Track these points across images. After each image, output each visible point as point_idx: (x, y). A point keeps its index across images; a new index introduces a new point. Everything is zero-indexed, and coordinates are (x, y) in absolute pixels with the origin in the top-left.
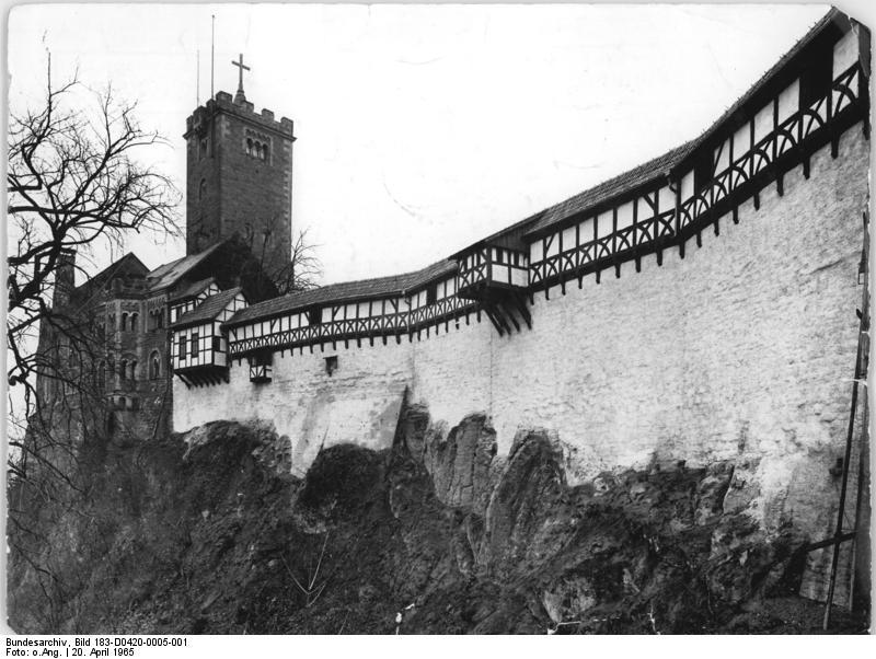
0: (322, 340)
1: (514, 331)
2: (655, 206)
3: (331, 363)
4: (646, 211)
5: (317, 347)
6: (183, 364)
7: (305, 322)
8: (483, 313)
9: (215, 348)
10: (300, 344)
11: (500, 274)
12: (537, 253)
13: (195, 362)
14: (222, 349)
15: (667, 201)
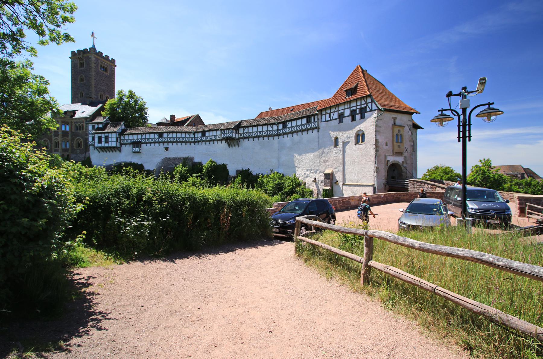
0: (163, 143)
1: (234, 147)
2: (273, 128)
3: (167, 149)
4: (270, 128)
5: (161, 144)
6: (100, 145)
7: (156, 136)
8: (224, 142)
9: (117, 141)
10: (155, 143)
11: (234, 135)
12: (241, 130)
13: (107, 145)
14: (119, 141)
15: (275, 127)
